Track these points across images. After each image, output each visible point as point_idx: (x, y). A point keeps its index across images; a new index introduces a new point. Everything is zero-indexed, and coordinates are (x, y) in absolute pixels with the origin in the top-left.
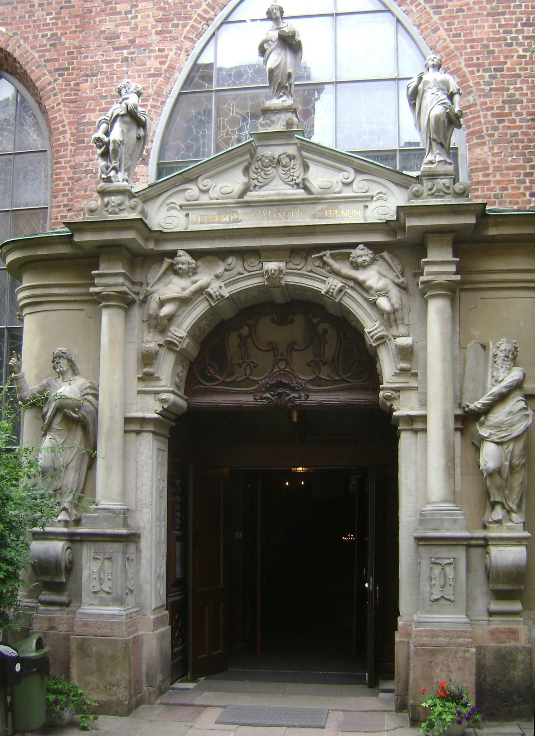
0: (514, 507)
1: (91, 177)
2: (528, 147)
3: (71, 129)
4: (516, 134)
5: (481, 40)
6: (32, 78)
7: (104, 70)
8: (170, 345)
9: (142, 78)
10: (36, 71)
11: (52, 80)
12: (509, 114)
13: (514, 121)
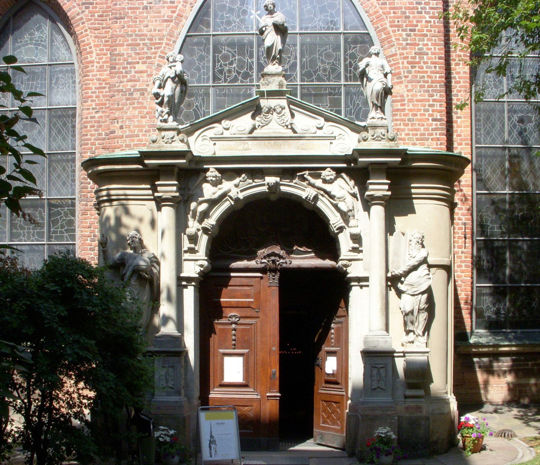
0: (421, 334)
1: (122, 95)
2: (431, 87)
3: (96, 50)
4: (423, 77)
5: (401, 8)
6: (64, 9)
7: (130, 15)
9: (158, 22)
10: (68, 3)
11: (80, 11)
12: (419, 63)
13: (422, 68)
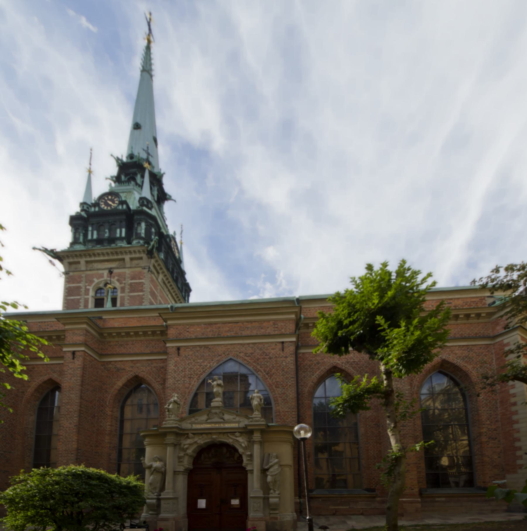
8: (187, 455)
